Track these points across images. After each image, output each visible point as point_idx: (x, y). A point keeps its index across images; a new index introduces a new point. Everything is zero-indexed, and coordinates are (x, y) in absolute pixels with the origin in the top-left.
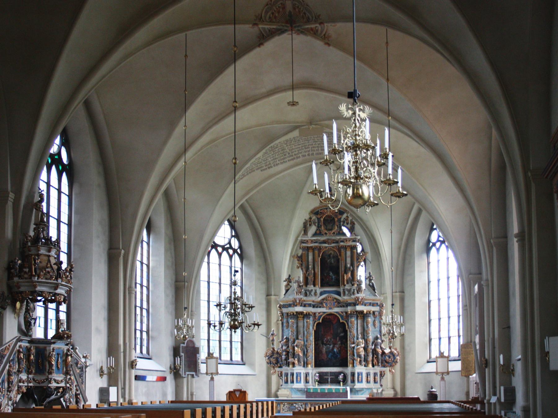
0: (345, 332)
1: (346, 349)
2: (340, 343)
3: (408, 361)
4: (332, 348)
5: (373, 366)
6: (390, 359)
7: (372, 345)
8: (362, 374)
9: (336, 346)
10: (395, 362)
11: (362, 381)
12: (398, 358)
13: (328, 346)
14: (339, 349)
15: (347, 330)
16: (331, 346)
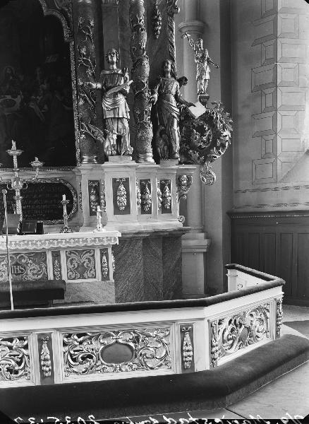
0: (62, 50)
1: (69, 108)
2: (45, 86)
3: (248, 150)
4: (22, 103)
5: (157, 159)
6: (204, 138)
7: (153, 93)
8: (126, 183)
9: (33, 97)
10: (218, 149)
11: (127, 210)
12: (227, 133)
13: (9, 97)
14: (46, 107)
15: (68, 44)
16: (18, 100)
